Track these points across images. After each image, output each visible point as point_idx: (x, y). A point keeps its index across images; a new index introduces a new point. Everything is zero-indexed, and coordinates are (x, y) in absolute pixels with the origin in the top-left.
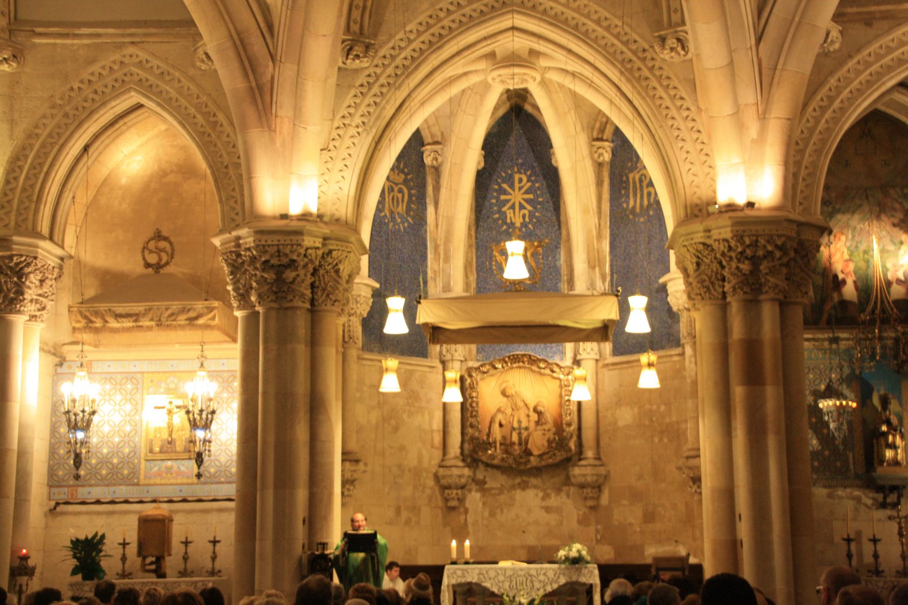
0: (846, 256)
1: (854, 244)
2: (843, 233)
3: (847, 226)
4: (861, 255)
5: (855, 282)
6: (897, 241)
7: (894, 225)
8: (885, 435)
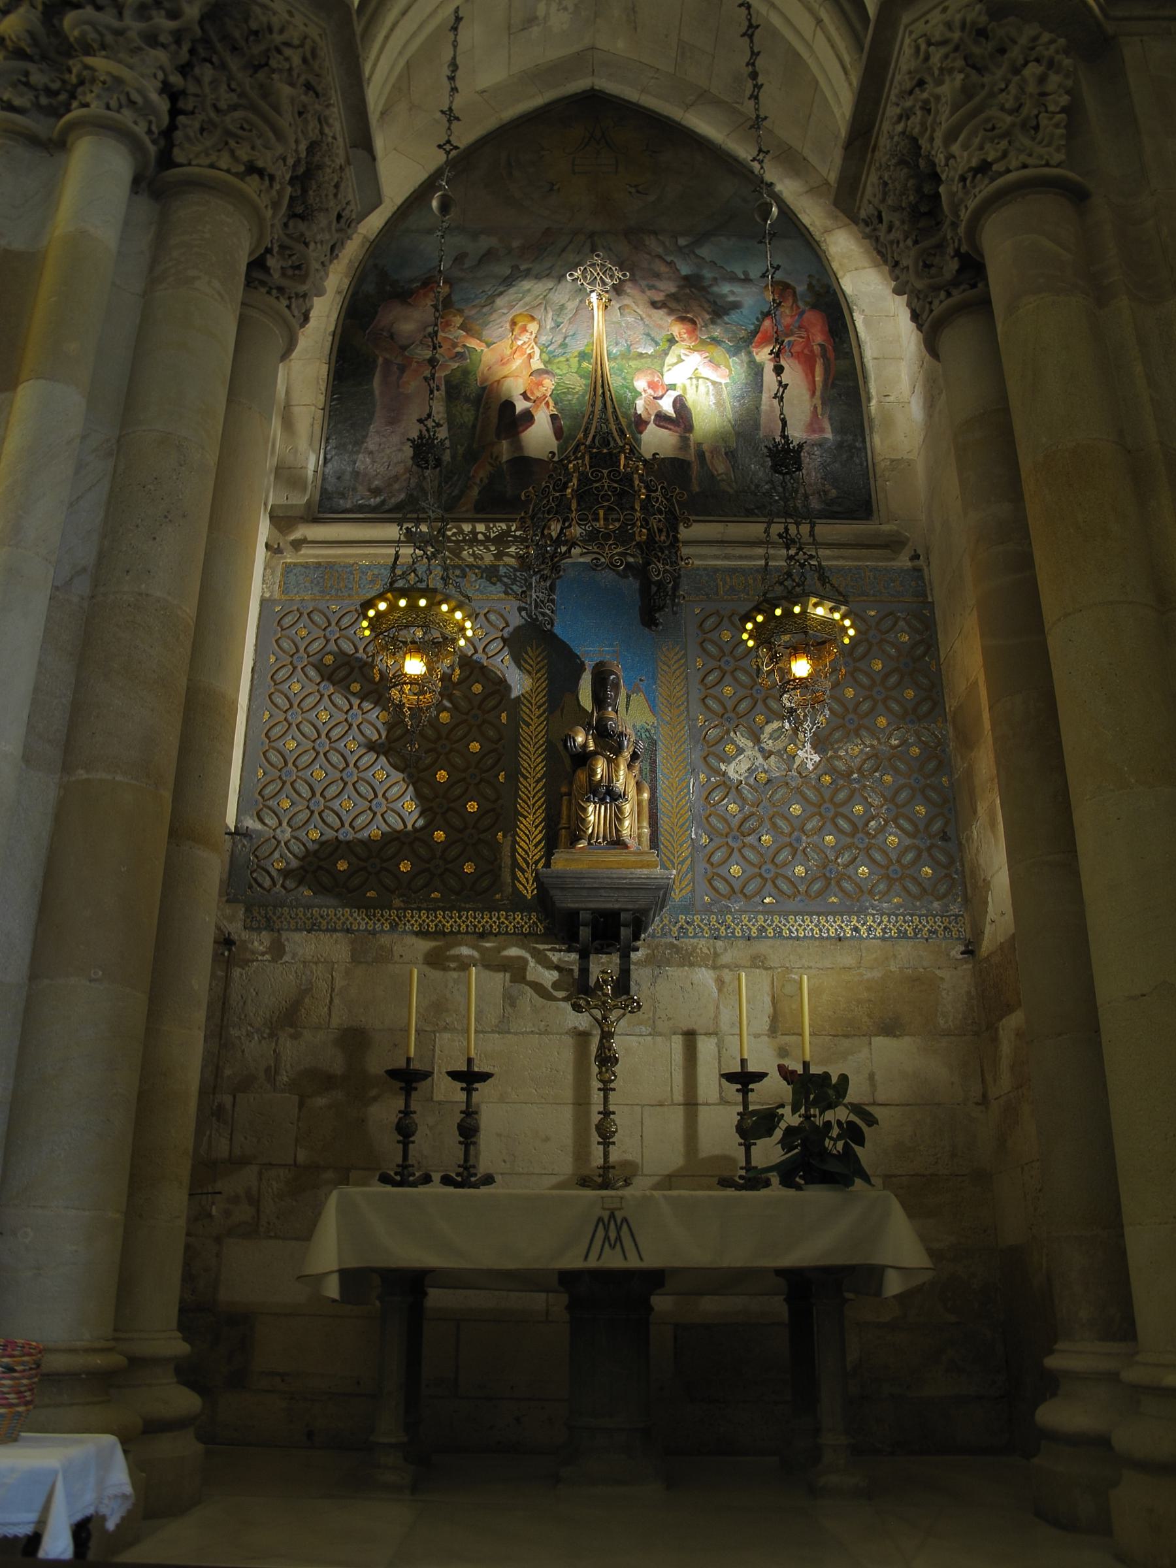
0: (537, 364)
1: (559, 339)
2: (533, 318)
3: (545, 303)
4: (574, 362)
5: (553, 417)
6: (661, 336)
7: (654, 305)
8: (583, 759)
